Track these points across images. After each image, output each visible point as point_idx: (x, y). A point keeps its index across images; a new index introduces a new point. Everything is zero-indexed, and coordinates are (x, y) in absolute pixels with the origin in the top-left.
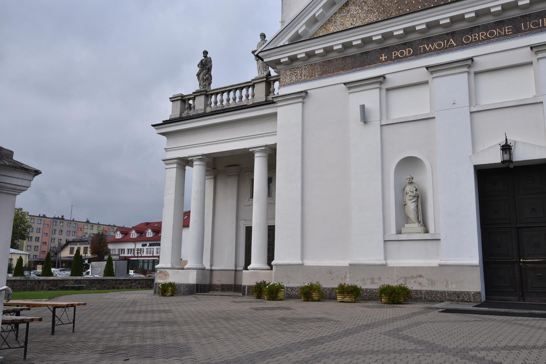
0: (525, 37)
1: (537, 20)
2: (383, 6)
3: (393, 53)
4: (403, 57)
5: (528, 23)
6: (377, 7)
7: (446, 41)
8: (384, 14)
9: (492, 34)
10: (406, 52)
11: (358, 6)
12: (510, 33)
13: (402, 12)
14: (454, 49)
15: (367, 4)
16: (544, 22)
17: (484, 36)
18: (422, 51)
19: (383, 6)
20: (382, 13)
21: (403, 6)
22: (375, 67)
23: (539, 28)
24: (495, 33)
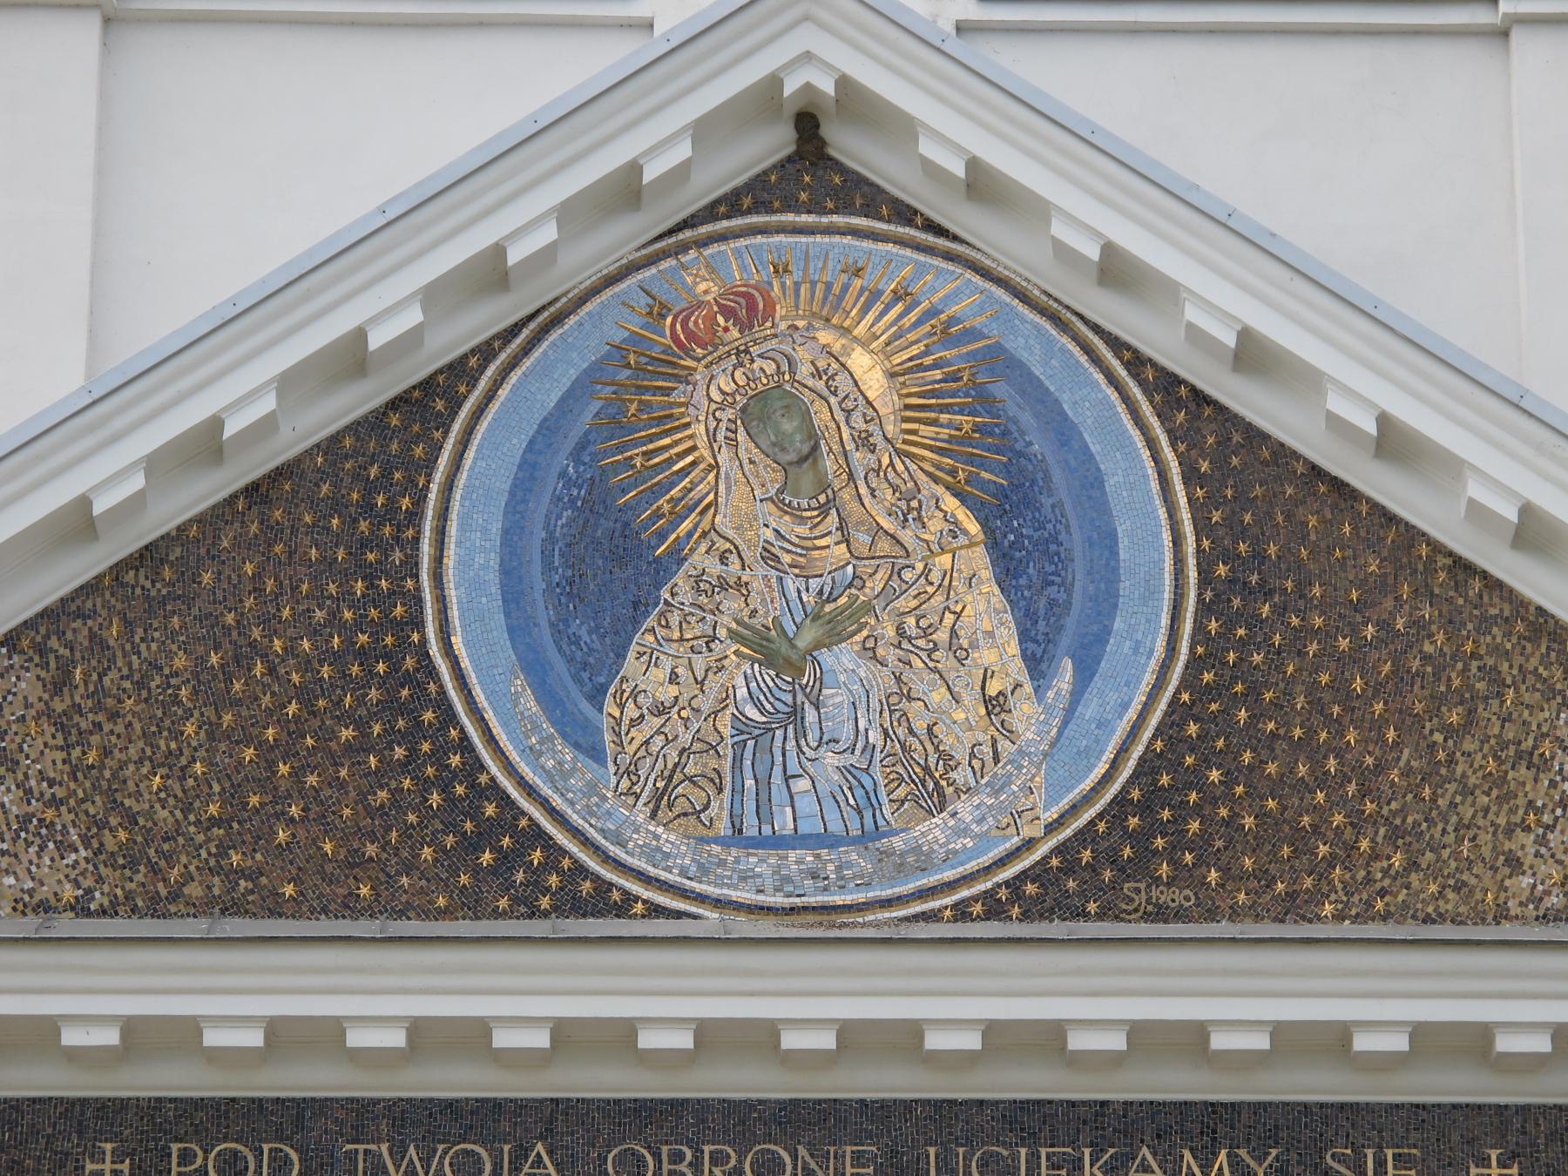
1: (1004, 1144)
2: (131, 819)
3: (175, 1147)
6: (87, 813)
7: (506, 1148)
8: (127, 872)
13: (252, 892)
15: (20, 776)
16: (1039, 1167)
19: (131, 819)
20: (121, 861)
21: (258, 856)
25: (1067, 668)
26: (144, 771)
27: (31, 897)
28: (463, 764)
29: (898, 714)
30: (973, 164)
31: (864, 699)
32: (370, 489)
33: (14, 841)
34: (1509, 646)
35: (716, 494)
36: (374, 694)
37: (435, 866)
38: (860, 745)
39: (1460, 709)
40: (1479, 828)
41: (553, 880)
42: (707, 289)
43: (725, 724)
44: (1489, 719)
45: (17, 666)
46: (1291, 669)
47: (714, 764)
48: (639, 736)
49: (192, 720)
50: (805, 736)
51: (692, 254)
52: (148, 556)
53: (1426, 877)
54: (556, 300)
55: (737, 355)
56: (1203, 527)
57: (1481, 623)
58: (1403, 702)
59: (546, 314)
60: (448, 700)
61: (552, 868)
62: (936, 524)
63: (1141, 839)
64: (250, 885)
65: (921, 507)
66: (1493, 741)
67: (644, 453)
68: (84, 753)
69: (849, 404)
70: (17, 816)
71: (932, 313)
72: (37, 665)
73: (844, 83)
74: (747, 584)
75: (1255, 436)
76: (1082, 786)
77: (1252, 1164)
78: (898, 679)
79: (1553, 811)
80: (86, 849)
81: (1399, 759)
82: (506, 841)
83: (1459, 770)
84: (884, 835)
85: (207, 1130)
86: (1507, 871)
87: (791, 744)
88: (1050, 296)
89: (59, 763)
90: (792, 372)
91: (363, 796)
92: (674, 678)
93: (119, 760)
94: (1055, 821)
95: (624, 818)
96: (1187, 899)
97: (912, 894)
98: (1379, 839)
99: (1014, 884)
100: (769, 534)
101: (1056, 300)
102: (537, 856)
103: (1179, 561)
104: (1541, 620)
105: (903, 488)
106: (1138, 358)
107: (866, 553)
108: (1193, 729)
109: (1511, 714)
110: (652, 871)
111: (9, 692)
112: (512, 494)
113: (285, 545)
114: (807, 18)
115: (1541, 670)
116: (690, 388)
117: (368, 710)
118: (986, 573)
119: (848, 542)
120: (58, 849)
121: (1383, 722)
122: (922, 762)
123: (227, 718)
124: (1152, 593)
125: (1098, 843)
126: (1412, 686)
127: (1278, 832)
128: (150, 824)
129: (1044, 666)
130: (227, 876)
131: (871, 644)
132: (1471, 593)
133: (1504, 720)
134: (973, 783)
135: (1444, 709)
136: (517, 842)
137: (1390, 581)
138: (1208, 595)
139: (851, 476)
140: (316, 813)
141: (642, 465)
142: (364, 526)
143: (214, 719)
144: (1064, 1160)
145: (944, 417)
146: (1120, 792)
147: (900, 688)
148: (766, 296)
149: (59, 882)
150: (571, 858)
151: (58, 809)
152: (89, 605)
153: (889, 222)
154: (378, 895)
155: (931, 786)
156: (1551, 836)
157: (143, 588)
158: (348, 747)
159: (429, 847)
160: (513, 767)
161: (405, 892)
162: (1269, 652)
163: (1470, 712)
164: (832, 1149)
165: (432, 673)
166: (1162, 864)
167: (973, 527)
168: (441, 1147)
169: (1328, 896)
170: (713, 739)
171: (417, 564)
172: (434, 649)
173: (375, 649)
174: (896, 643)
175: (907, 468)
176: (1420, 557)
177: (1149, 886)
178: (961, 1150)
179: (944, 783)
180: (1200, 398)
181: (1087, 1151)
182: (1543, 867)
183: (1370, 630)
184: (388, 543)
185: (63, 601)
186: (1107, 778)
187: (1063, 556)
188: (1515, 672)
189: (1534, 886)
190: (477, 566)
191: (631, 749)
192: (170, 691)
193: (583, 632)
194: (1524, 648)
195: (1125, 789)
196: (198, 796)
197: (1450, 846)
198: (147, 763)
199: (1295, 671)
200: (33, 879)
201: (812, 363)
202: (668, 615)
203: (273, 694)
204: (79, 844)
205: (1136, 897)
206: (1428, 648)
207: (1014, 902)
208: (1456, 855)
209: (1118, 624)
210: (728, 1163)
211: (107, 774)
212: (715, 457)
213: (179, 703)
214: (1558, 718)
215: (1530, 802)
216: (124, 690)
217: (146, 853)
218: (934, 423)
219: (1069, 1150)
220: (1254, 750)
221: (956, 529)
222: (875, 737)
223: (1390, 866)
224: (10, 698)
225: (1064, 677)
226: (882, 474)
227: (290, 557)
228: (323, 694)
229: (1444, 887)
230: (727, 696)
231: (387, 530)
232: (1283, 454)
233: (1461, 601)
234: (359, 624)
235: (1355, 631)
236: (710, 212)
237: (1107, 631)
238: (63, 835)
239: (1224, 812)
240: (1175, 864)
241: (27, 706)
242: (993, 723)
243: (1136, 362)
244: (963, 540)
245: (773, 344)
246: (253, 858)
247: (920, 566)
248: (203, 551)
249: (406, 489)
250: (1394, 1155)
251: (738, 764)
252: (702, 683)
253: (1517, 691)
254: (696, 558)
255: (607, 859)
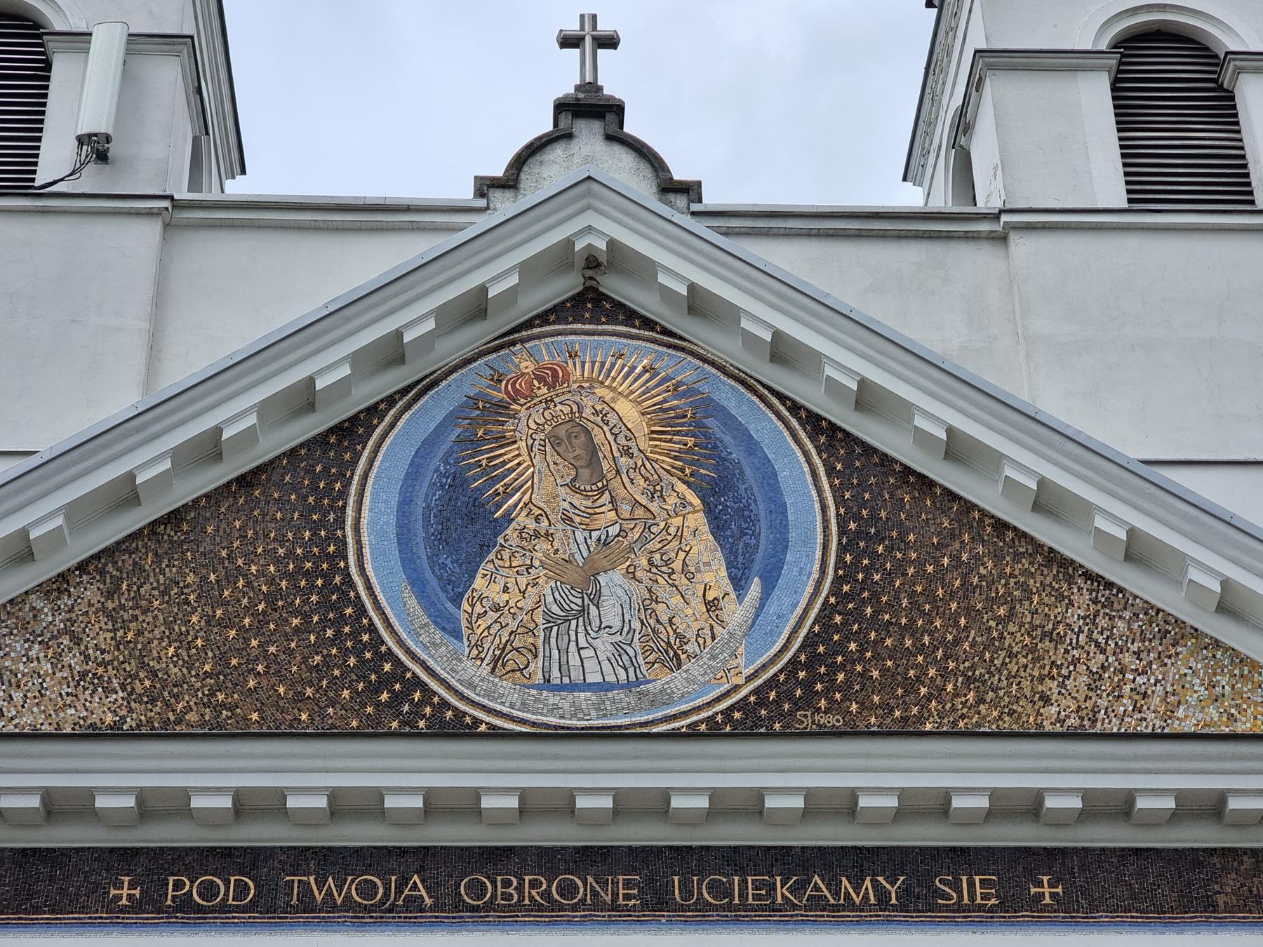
0: (682, 930)
1: (723, 874)
3: (171, 879)
4: (211, 910)
5: (695, 878)
6: (125, 670)
7: (394, 878)
8: (149, 706)
9: (568, 890)
10: (225, 889)
11: (40, 643)
12: (631, 903)
13: (230, 718)
14: (421, 917)
15: (83, 648)
16: (747, 888)
17: (538, 893)
18: (294, 901)
20: (145, 699)
21: (236, 696)
22: (81, 924)
23: (730, 907)
24: (581, 890)
25: (755, 587)
26: (164, 644)
27: (85, 721)
28: (370, 639)
29: (650, 611)
30: (692, 287)
31: (628, 602)
32: (315, 479)
33: (76, 687)
34: (1033, 570)
35: (533, 481)
36: (314, 598)
37: (351, 702)
38: (626, 630)
39: (1005, 606)
40: (1022, 677)
41: (428, 710)
42: (528, 366)
43: (539, 616)
44: (1023, 613)
45: (85, 582)
46: (897, 584)
47: (531, 640)
48: (483, 624)
49: (197, 614)
50: (590, 624)
51: (518, 346)
52: (174, 518)
53: (990, 707)
54: (435, 372)
55: (546, 403)
56: (839, 501)
57: (1014, 556)
58: (969, 602)
59: (428, 380)
60: (361, 602)
61: (426, 703)
62: (672, 500)
63: (808, 685)
64: (229, 714)
65: (662, 489)
66: (1027, 626)
67: (488, 458)
68: (125, 633)
69: (616, 431)
70: (79, 672)
71: (666, 379)
72: (98, 581)
73: (612, 243)
74: (552, 534)
75: (869, 450)
76: (768, 654)
77: (888, 886)
78: (650, 591)
79: (1068, 667)
80: (123, 692)
81: (968, 636)
82: (397, 686)
83: (1007, 644)
84: (642, 683)
85: (193, 867)
86: (1041, 703)
87: (581, 629)
88: (740, 370)
89: (109, 641)
90: (580, 412)
91: (305, 659)
92: (506, 589)
93: (148, 638)
94: (752, 674)
95: (474, 673)
96: (838, 721)
97: (661, 719)
98: (959, 685)
99: (727, 713)
100: (566, 505)
101: (744, 373)
102: (417, 696)
103: (826, 521)
104: (1052, 555)
105: (651, 479)
106: (795, 405)
107: (628, 516)
108: (838, 619)
109: (1037, 610)
110: (491, 704)
111: (79, 597)
112: (405, 480)
113: (261, 511)
114: (589, 207)
115: (1054, 584)
116: (517, 421)
117: (310, 607)
118: (705, 527)
119: (616, 510)
120: (104, 691)
121: (957, 615)
122: (666, 640)
123: (219, 613)
124: (809, 540)
125: (780, 688)
126: (974, 593)
127: (894, 680)
128: (165, 677)
129: (743, 583)
130: (214, 708)
131: (631, 570)
132: (1007, 539)
133: (1033, 614)
134: (698, 652)
135: (995, 607)
136: (404, 687)
137: (957, 532)
138: (844, 540)
139: (618, 472)
140: (275, 669)
141: (486, 465)
142: (311, 499)
143: (211, 613)
144: (763, 884)
145: (676, 438)
146: (793, 657)
147: (651, 596)
148: (564, 370)
149: (104, 712)
150: (439, 697)
151: (106, 667)
152: (134, 545)
153: (639, 329)
154: (313, 719)
155: (672, 654)
156: (1067, 682)
157: (169, 535)
158: (297, 630)
159: (347, 690)
160: (402, 641)
161: (331, 718)
162: (883, 574)
163: (1011, 609)
164: (610, 878)
165: (352, 586)
166: (821, 700)
167: (696, 502)
168: (350, 878)
169: (928, 719)
170: (532, 626)
171: (344, 522)
172: (353, 571)
173: (316, 572)
174: (648, 569)
175: (653, 467)
176: (974, 518)
177: (813, 714)
178: (695, 878)
179: (680, 652)
180: (834, 427)
181: (778, 879)
182: (1064, 701)
183: (946, 561)
184: (326, 509)
185: (118, 543)
186: (785, 648)
187: (753, 518)
188: (1038, 585)
189: (1059, 712)
190: (382, 523)
191: (479, 631)
192: (183, 597)
193: (448, 562)
194: (1042, 571)
195: (796, 656)
196: (198, 660)
197: (1004, 689)
198: (166, 639)
199: (901, 584)
200: (87, 710)
201: (593, 407)
202: (503, 552)
203: (250, 598)
204: (118, 688)
205: (805, 721)
206: (982, 571)
207: (726, 724)
208: (1008, 693)
209: (789, 557)
210: (541, 887)
211: (139, 646)
212: (532, 460)
213: (188, 603)
214: (1067, 612)
215: (1053, 662)
216: (154, 597)
217: (162, 694)
218: (670, 441)
219: (767, 878)
220: (876, 631)
221: (684, 503)
222: (636, 625)
223: (967, 701)
224: (79, 601)
225: (755, 587)
226: (637, 471)
227: (263, 518)
228: (282, 598)
229: (1002, 713)
230: (540, 601)
231: (326, 502)
232: (886, 460)
233: (1001, 544)
234: (306, 557)
235: (937, 562)
236: (529, 324)
237: (782, 562)
238: (108, 683)
239: (859, 668)
240: (831, 700)
241: (90, 605)
242: (711, 617)
243: (795, 408)
244: (689, 508)
245: (568, 396)
246: (232, 697)
247: (662, 524)
248: (208, 514)
249: (338, 479)
250: (980, 879)
251: (547, 641)
252: (524, 592)
253: (1040, 595)
254: (520, 519)
255: (462, 697)
